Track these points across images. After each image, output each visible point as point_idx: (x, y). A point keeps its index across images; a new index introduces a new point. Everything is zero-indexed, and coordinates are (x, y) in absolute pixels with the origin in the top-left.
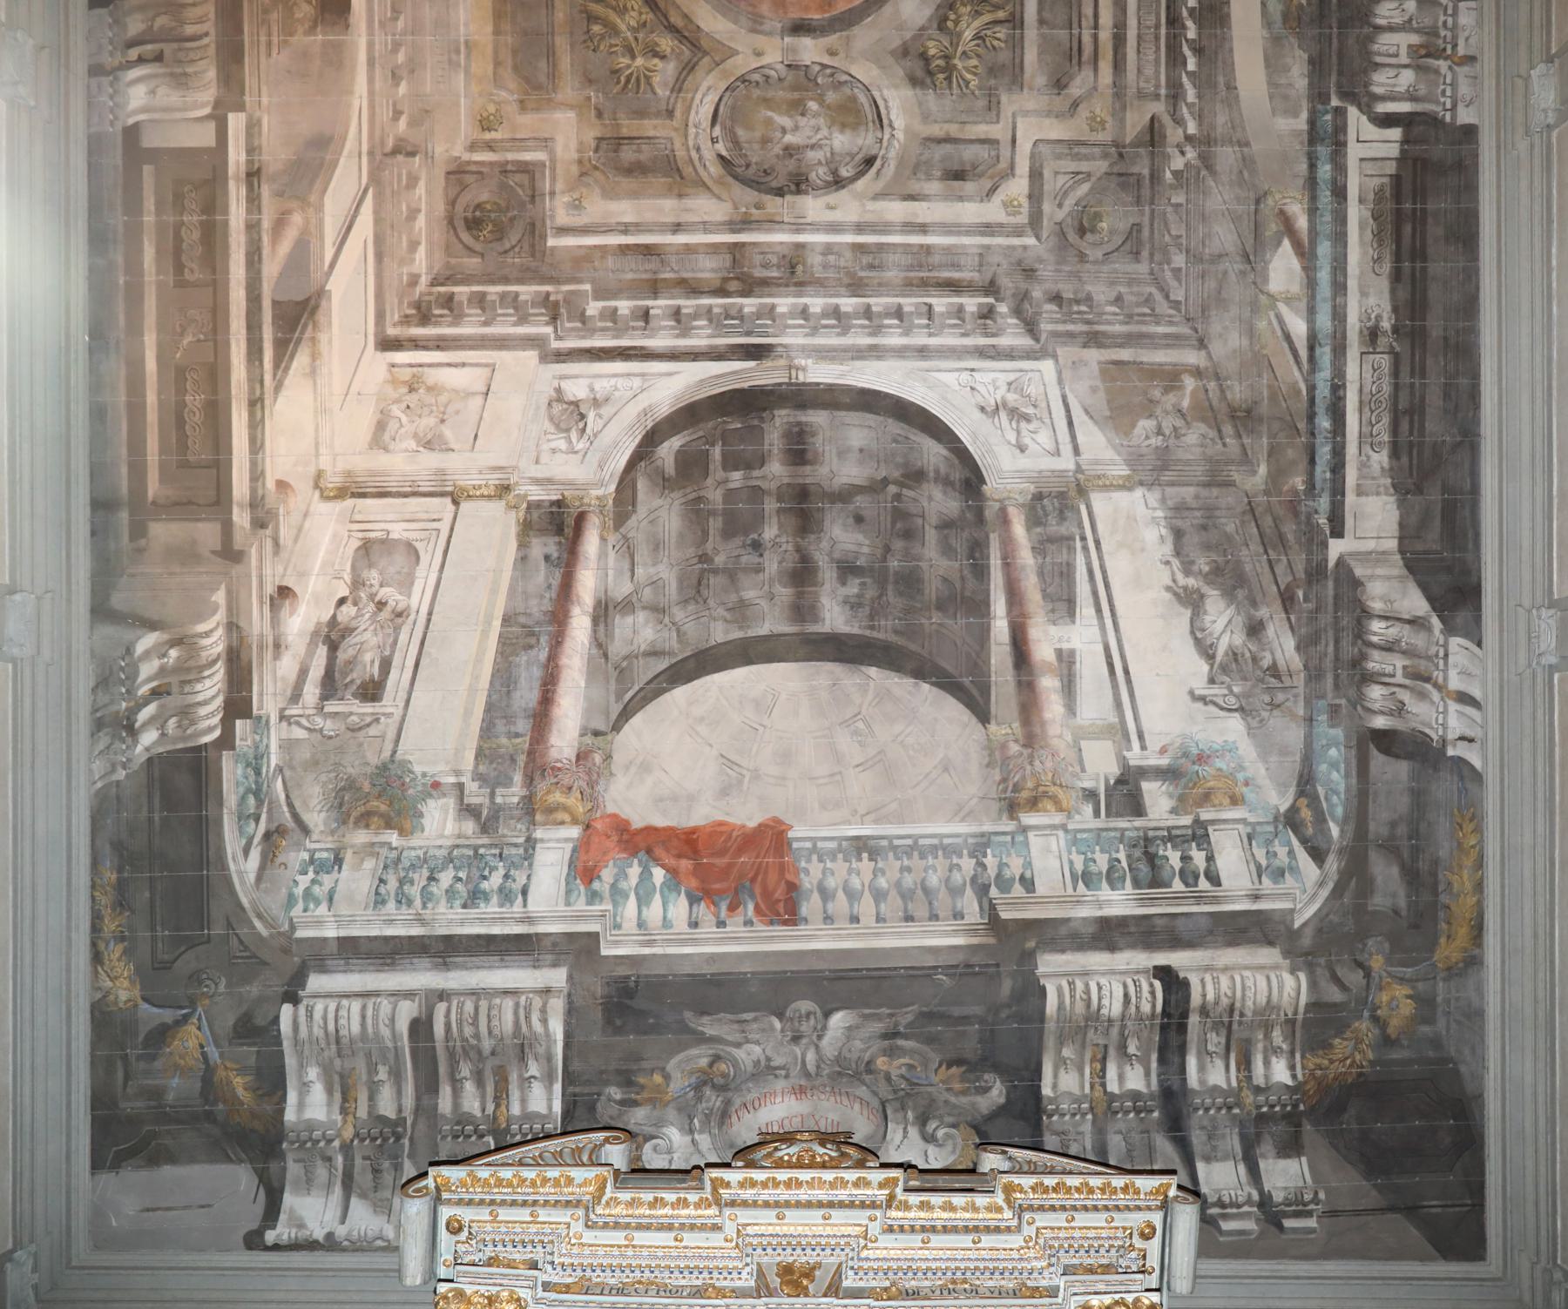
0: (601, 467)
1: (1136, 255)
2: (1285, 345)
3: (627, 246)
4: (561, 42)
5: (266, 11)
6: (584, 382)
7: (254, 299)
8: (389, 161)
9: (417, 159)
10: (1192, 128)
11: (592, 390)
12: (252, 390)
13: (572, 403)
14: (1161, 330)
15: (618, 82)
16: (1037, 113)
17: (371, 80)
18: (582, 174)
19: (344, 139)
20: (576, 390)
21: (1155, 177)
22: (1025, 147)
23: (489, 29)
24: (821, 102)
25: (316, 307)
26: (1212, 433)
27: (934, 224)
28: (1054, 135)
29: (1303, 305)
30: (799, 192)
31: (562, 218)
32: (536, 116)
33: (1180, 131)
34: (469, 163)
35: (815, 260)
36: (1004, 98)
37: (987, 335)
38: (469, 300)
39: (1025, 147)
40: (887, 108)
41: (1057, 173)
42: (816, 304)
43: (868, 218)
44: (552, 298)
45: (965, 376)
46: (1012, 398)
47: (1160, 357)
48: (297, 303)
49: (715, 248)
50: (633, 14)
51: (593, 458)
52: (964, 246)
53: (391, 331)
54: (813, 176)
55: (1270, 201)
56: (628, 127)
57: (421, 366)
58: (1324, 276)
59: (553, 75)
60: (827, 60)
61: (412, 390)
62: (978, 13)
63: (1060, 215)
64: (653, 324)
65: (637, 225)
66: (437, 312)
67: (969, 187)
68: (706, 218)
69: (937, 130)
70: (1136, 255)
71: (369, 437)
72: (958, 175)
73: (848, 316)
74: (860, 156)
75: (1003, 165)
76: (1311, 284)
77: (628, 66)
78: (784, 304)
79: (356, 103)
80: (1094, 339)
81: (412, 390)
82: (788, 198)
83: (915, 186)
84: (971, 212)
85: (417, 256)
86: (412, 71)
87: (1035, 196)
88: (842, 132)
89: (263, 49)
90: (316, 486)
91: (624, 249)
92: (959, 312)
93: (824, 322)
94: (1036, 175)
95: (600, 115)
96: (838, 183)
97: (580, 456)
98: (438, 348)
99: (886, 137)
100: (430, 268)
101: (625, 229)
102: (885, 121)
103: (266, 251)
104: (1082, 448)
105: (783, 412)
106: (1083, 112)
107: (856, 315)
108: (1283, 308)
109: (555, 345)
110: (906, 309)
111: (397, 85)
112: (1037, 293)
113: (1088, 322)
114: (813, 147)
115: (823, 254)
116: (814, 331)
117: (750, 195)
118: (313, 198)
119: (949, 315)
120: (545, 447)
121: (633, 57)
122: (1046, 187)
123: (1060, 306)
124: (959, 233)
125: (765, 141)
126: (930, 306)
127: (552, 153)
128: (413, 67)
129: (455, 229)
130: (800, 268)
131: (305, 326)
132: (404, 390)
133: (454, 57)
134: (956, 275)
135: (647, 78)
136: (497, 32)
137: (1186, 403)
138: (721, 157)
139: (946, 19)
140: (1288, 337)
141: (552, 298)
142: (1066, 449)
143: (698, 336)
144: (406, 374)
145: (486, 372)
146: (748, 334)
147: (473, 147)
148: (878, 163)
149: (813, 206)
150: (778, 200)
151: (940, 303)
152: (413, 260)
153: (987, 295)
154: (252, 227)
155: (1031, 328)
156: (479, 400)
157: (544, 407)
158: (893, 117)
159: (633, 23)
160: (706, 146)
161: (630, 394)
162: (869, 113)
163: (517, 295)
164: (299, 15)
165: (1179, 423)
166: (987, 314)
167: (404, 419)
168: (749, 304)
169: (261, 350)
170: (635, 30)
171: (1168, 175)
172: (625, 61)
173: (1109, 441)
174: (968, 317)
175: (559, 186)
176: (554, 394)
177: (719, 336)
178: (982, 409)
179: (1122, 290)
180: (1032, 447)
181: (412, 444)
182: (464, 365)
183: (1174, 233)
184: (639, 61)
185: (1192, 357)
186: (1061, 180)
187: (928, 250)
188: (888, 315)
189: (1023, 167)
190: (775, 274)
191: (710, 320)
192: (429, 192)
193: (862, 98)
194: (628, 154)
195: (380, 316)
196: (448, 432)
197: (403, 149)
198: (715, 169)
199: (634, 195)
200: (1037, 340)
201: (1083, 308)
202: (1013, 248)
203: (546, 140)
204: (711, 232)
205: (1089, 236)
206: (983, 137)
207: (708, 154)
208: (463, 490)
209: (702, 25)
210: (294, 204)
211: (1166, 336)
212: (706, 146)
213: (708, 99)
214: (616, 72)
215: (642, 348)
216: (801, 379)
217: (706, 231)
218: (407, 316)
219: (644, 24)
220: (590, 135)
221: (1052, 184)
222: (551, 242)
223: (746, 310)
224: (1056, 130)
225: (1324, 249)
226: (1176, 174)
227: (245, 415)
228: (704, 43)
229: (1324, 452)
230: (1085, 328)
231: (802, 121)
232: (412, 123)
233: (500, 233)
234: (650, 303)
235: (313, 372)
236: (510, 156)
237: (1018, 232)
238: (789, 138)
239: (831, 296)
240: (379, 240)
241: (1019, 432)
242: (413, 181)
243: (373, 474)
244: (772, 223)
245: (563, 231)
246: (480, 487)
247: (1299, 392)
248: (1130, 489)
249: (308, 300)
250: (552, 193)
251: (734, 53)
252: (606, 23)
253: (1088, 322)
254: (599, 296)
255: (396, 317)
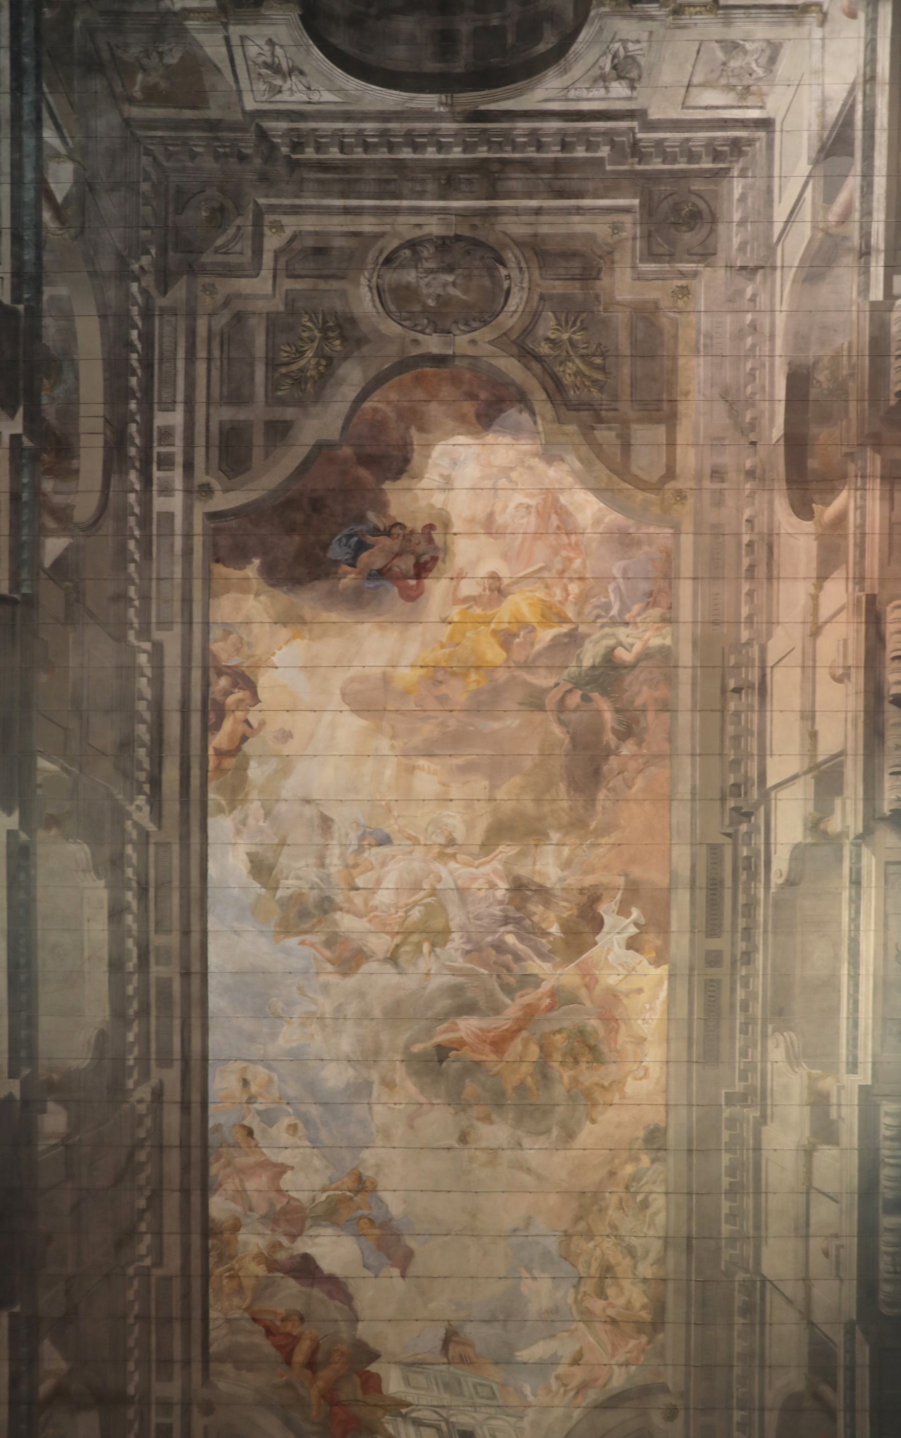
0: (601, 29)
1: (179, 191)
2: (60, 121)
3: (577, 197)
4: (625, 348)
5: (851, 375)
6: (613, 94)
7: (868, 158)
8: (761, 264)
9: (738, 265)
10: (134, 287)
11: (606, 88)
12: (873, 89)
13: (623, 78)
14: (160, 133)
15: (582, 321)
16: (256, 297)
17: (773, 324)
18: (611, 253)
19: (794, 281)
20: (619, 89)
21: (163, 250)
22: (266, 273)
23: (681, 361)
24: (424, 305)
25: (820, 151)
26: (119, 53)
27: (338, 214)
28: (243, 281)
29: (46, 152)
30: (443, 238)
31: (627, 219)
32: (647, 297)
33: (143, 284)
34: (699, 262)
35: (431, 187)
36: (282, 308)
37: (298, 130)
38: (701, 157)
39: (266, 273)
40: (373, 301)
41: (241, 253)
42: (431, 154)
43: (389, 219)
44: (636, 159)
45: (315, 97)
46: (278, 82)
47: (159, 113)
48: (834, 155)
49: (509, 195)
50: (569, 371)
51: (606, 36)
52: (314, 198)
53: (762, 134)
54: (432, 250)
55: (72, 231)
56: (575, 289)
57: (740, 107)
58: (29, 175)
59: (632, 328)
60: (420, 336)
61: (747, 88)
62: (301, 370)
63: (238, 221)
64: (559, 139)
65: (570, 214)
66: (726, 148)
67: (310, 242)
68: (515, 219)
69: (335, 284)
70: (179, 191)
71: (782, 51)
72: (319, 251)
73: (407, 145)
74: (395, 265)
75: (283, 260)
76: (40, 169)
77: (574, 333)
78: (457, 154)
79: (785, 308)
80: (213, 126)
81: (747, 88)
82: (452, 234)
83: (351, 243)
84: (309, 223)
85: (740, 190)
86: (741, 331)
87: (258, 237)
88: (409, 283)
89: (854, 353)
90: (825, 15)
91: (580, 195)
92: (319, 148)
93: (424, 140)
94: (258, 251)
95: (597, 297)
96: (413, 245)
97: (618, 37)
98: (726, 121)
99: (374, 280)
100: (731, 183)
101: (579, 210)
102: (375, 291)
103: (857, 194)
104: (223, 42)
105: (458, 70)
106: (219, 298)
107: (400, 145)
108: (62, 150)
109: (635, 124)
110: (360, 150)
111: (752, 321)
112: (258, 161)
113: (217, 139)
114: (431, 271)
115: (424, 191)
116: (432, 133)
117: (481, 235)
118: (820, 235)
119: (327, 145)
120: (644, 45)
121: (570, 339)
122: (250, 242)
123: (240, 152)
124: (319, 207)
125: (469, 277)
126: (342, 152)
127: (634, 267)
128: (739, 335)
129: (711, 211)
130: (443, 182)
131: (829, 138)
132: (753, 88)
133: (708, 341)
134: (321, 176)
135: (559, 324)
136: (674, 358)
137: (140, 77)
138: (504, 265)
139: (326, 366)
140: (58, 128)
141: (636, 159)
142: (235, 40)
143: (523, 129)
144: (751, 100)
145: (691, 102)
146: (484, 130)
147: (695, 274)
148: (381, 260)
149: (434, 227)
150: (459, 232)
151: (334, 153)
152: (743, 188)
153: (298, 160)
154: (867, 213)
155: (263, 135)
156: (695, 80)
157: (645, 75)
158: (369, 294)
159: (570, 365)
160: (515, 273)
161: (577, 85)
162: (387, 297)
163: (664, 162)
164: (826, 372)
165: (145, 61)
166: (297, 146)
167: (754, 66)
168: (483, 153)
169: (865, 119)
170: (569, 358)
171: (153, 251)
172: (576, 337)
173: (201, 47)
174: (312, 144)
175: (629, 244)
176: (637, 85)
177: (507, 129)
178: (302, 73)
179: (190, 164)
180: (262, 42)
181: (748, 46)
182: (706, 108)
183: (149, 208)
184: (565, 336)
185: (136, 112)
186: (238, 248)
187: (344, 195)
188: (375, 146)
189: (268, 259)
190: (462, 176)
191: (513, 141)
192: (730, 240)
193: (393, 308)
194: (576, 265)
195: (770, 145)
196: (720, 55)
197: (749, 271)
198: (509, 256)
199: (571, 236)
200: (258, 126)
201: (221, 150)
202: (277, 196)
203: (639, 279)
204: (512, 208)
205: (216, 205)
206: (299, 280)
207: (513, 265)
208: (710, 11)
209: (516, 362)
210: (833, 231)
211: (155, 129)
212: (515, 273)
213: (513, 309)
214: (583, 329)
215: (566, 121)
216: (443, 97)
217: (516, 209)
218: (750, 145)
219: (561, 363)
220: (605, 281)
221: (246, 246)
222: (636, 202)
223: (485, 148)
224: (244, 285)
225: (29, 195)
226: (147, 252)
227: (879, 69)
228: (515, 350)
229: (27, 38)
230: (220, 134)
231: (440, 291)
232: (741, 292)
233: (676, 209)
234: (560, 155)
235: (824, 102)
236: (666, 267)
237: (272, 209)
238: (450, 278)
239: (419, 160)
240: (769, 203)
241: (273, 55)
242: (742, 247)
243: (781, 24)
244: (465, 215)
245: (627, 210)
246: (696, 14)
247: (49, 86)
248: (184, 9)
249: (826, 157)
250: (634, 238)
251: (491, 342)
252: (591, 365)
253: (217, 139)
254: (600, 162)
255: (758, 145)
